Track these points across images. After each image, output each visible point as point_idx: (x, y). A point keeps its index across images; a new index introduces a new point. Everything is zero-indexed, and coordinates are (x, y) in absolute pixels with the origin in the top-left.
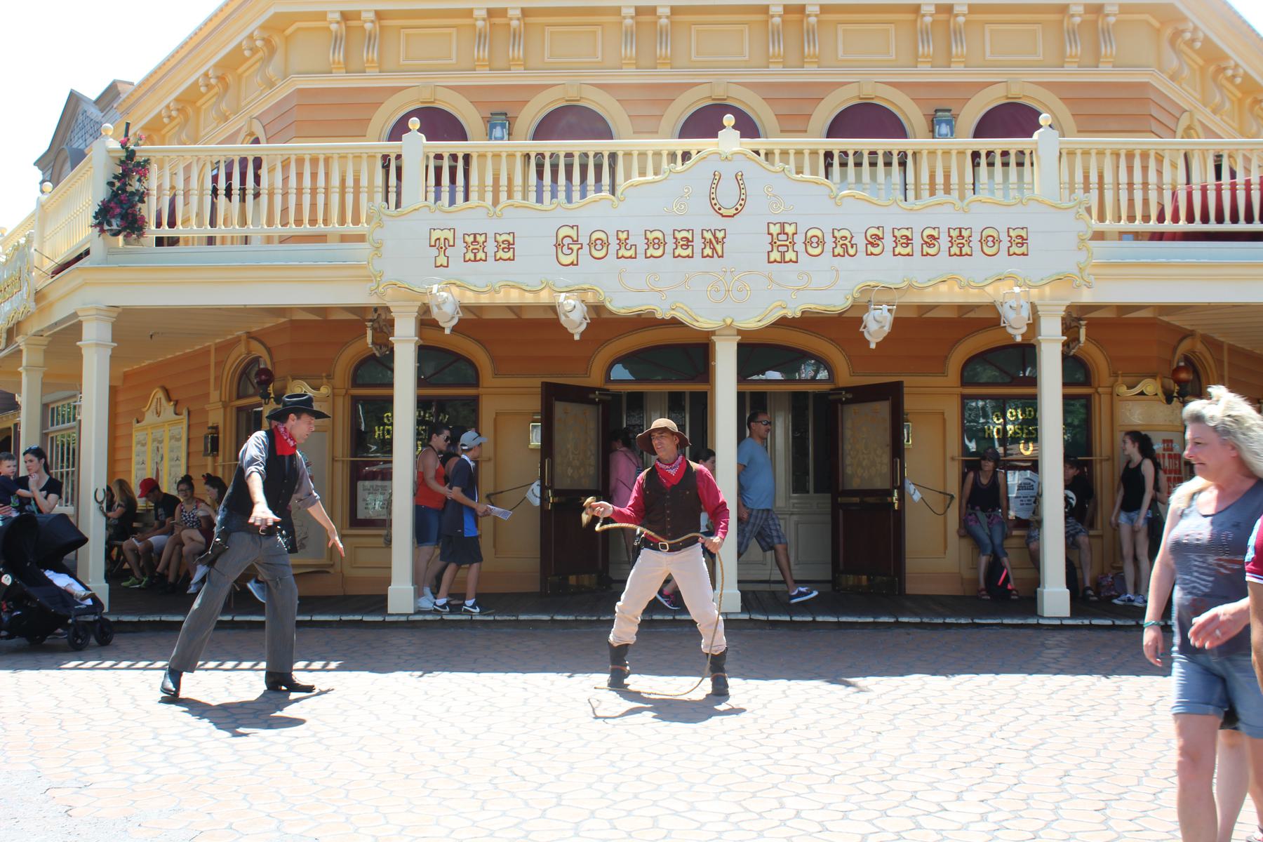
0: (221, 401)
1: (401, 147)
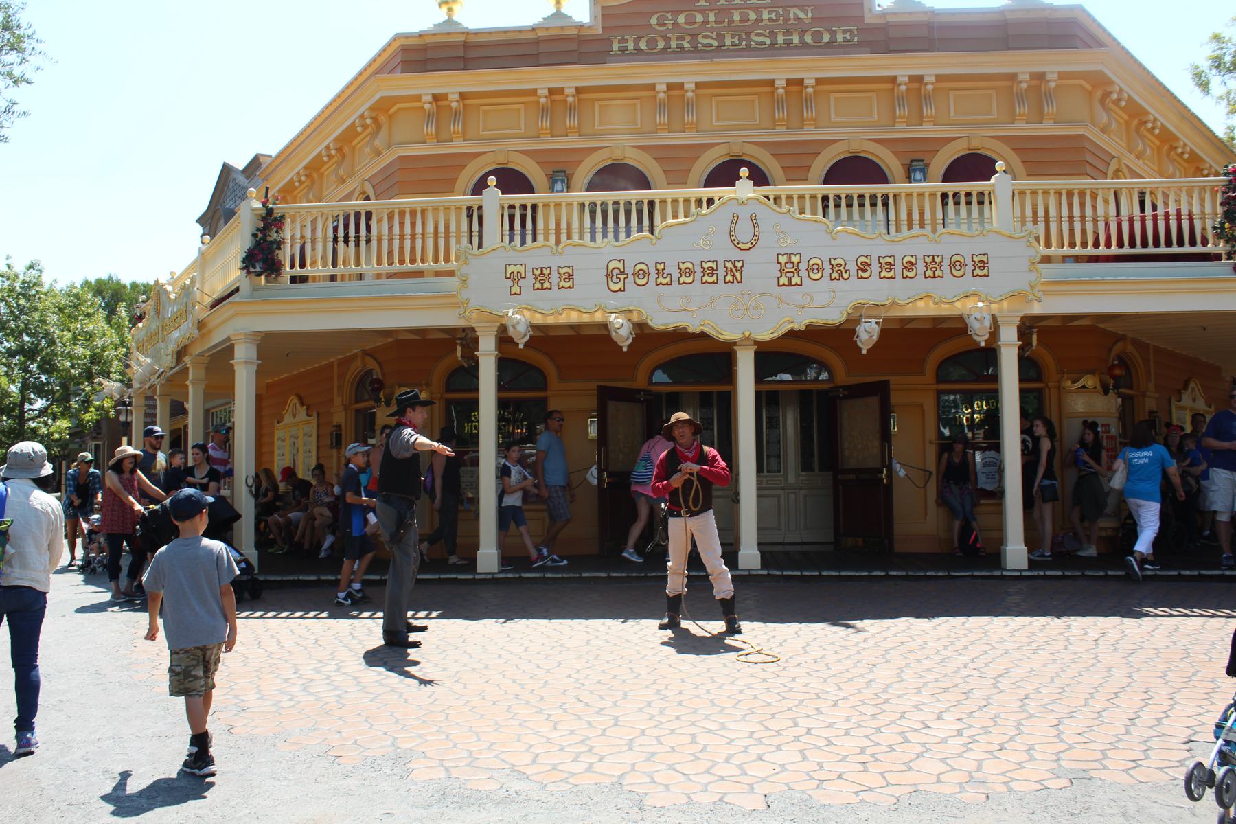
1: (481, 200)
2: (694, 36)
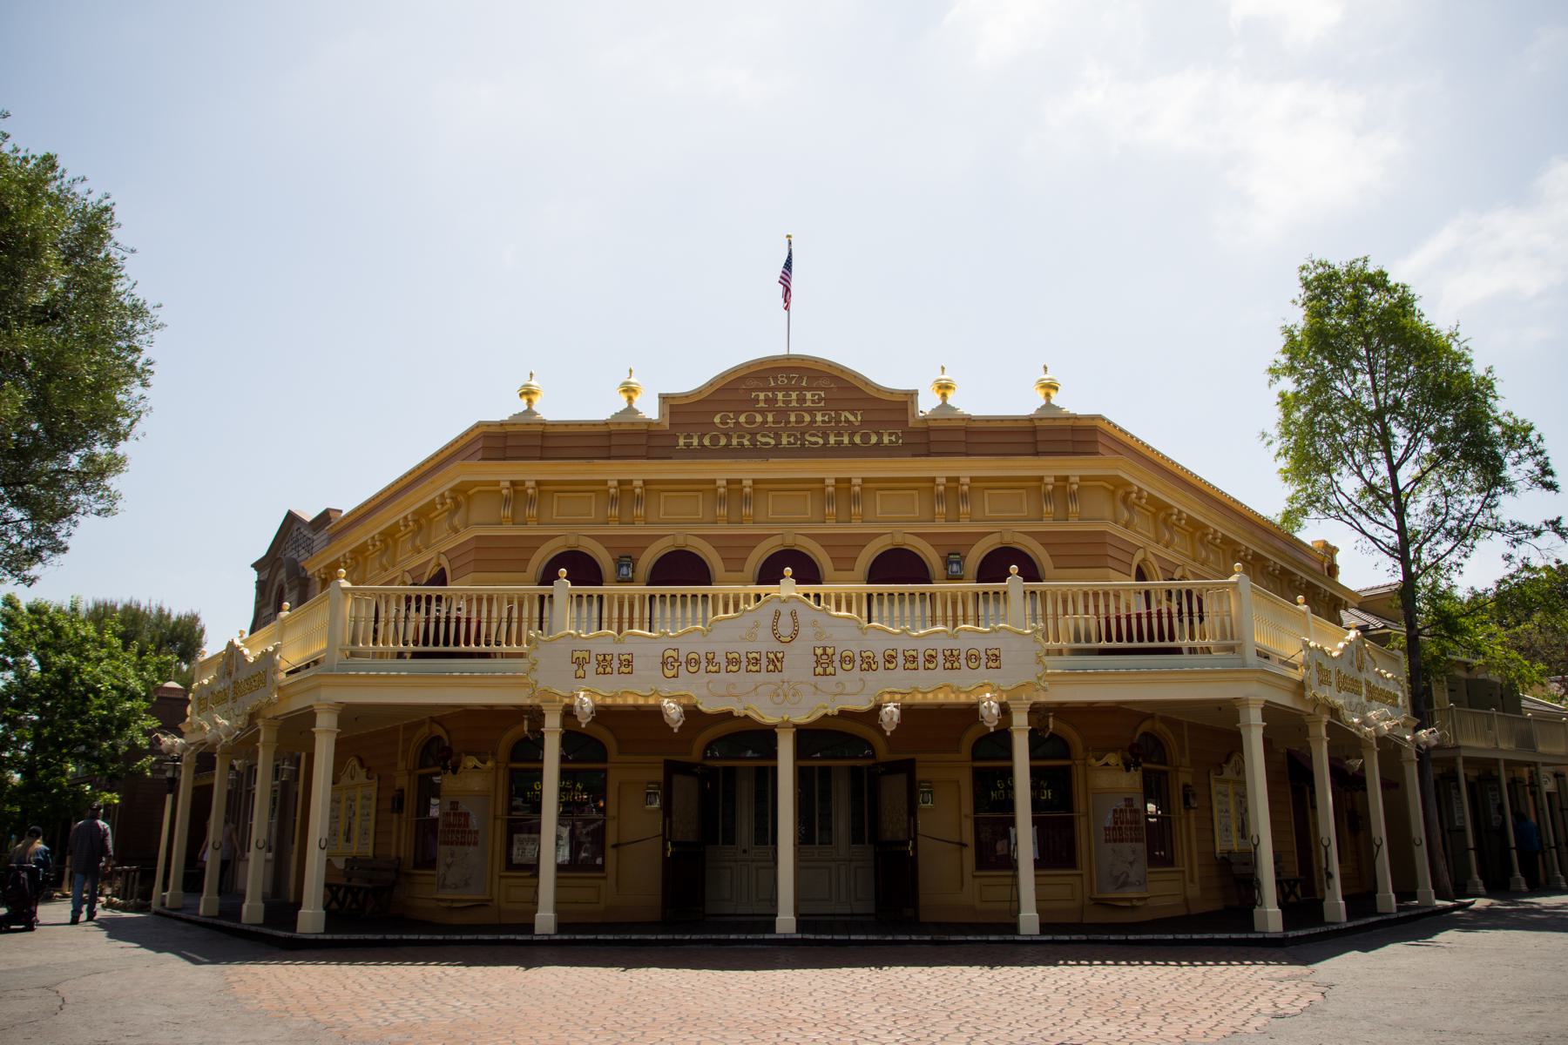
0: (406, 769)
1: (552, 590)
2: (753, 435)
